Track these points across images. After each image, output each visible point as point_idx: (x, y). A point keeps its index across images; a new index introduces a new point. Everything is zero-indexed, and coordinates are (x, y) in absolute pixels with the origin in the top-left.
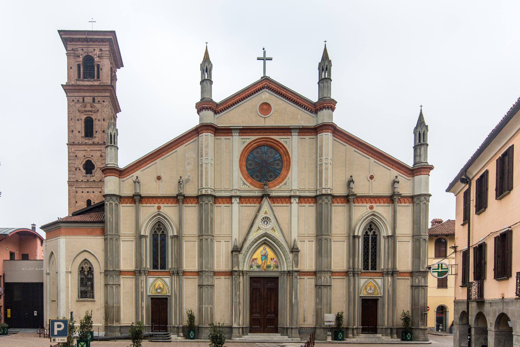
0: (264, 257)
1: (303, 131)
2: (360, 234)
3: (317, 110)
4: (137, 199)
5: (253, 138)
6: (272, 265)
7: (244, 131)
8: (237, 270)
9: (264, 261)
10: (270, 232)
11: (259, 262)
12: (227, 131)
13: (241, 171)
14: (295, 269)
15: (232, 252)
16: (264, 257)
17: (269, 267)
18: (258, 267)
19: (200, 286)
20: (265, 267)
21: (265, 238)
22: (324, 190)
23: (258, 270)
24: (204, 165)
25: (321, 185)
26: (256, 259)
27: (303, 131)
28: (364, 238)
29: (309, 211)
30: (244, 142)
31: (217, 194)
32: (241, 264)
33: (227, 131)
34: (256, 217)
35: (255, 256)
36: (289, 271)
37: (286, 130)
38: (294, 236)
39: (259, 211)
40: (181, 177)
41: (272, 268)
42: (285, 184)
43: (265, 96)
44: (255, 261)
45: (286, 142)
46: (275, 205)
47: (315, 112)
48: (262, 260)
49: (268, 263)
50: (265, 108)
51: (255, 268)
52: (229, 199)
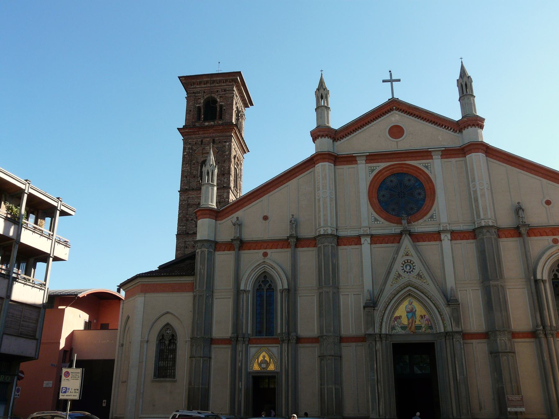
0: (410, 315)
1: (448, 153)
2: (545, 277)
3: (462, 129)
4: (240, 244)
5: (383, 165)
6: (423, 326)
7: (372, 158)
8: (373, 332)
9: (410, 321)
10: (414, 280)
11: (405, 321)
12: (350, 159)
13: (372, 204)
14: (455, 329)
15: (364, 307)
16: (410, 315)
17: (419, 327)
18: (404, 328)
19: (322, 357)
20: (413, 329)
21: (409, 288)
22: (483, 221)
23: (403, 332)
24: (321, 200)
25: (478, 216)
26: (400, 317)
27: (448, 153)
28: (553, 283)
29: (468, 249)
30: (373, 171)
31: (342, 233)
32: (377, 325)
33: (350, 159)
34: (394, 259)
35: (397, 314)
36: (447, 333)
37: (425, 154)
38: (450, 283)
39: (397, 252)
40: (293, 215)
41: (424, 329)
42: (432, 217)
43: (395, 118)
44: (398, 320)
45: (427, 167)
46: (420, 243)
47: (459, 131)
48: (408, 320)
49: (418, 323)
50: (396, 132)
51: (399, 330)
52: (357, 240)
